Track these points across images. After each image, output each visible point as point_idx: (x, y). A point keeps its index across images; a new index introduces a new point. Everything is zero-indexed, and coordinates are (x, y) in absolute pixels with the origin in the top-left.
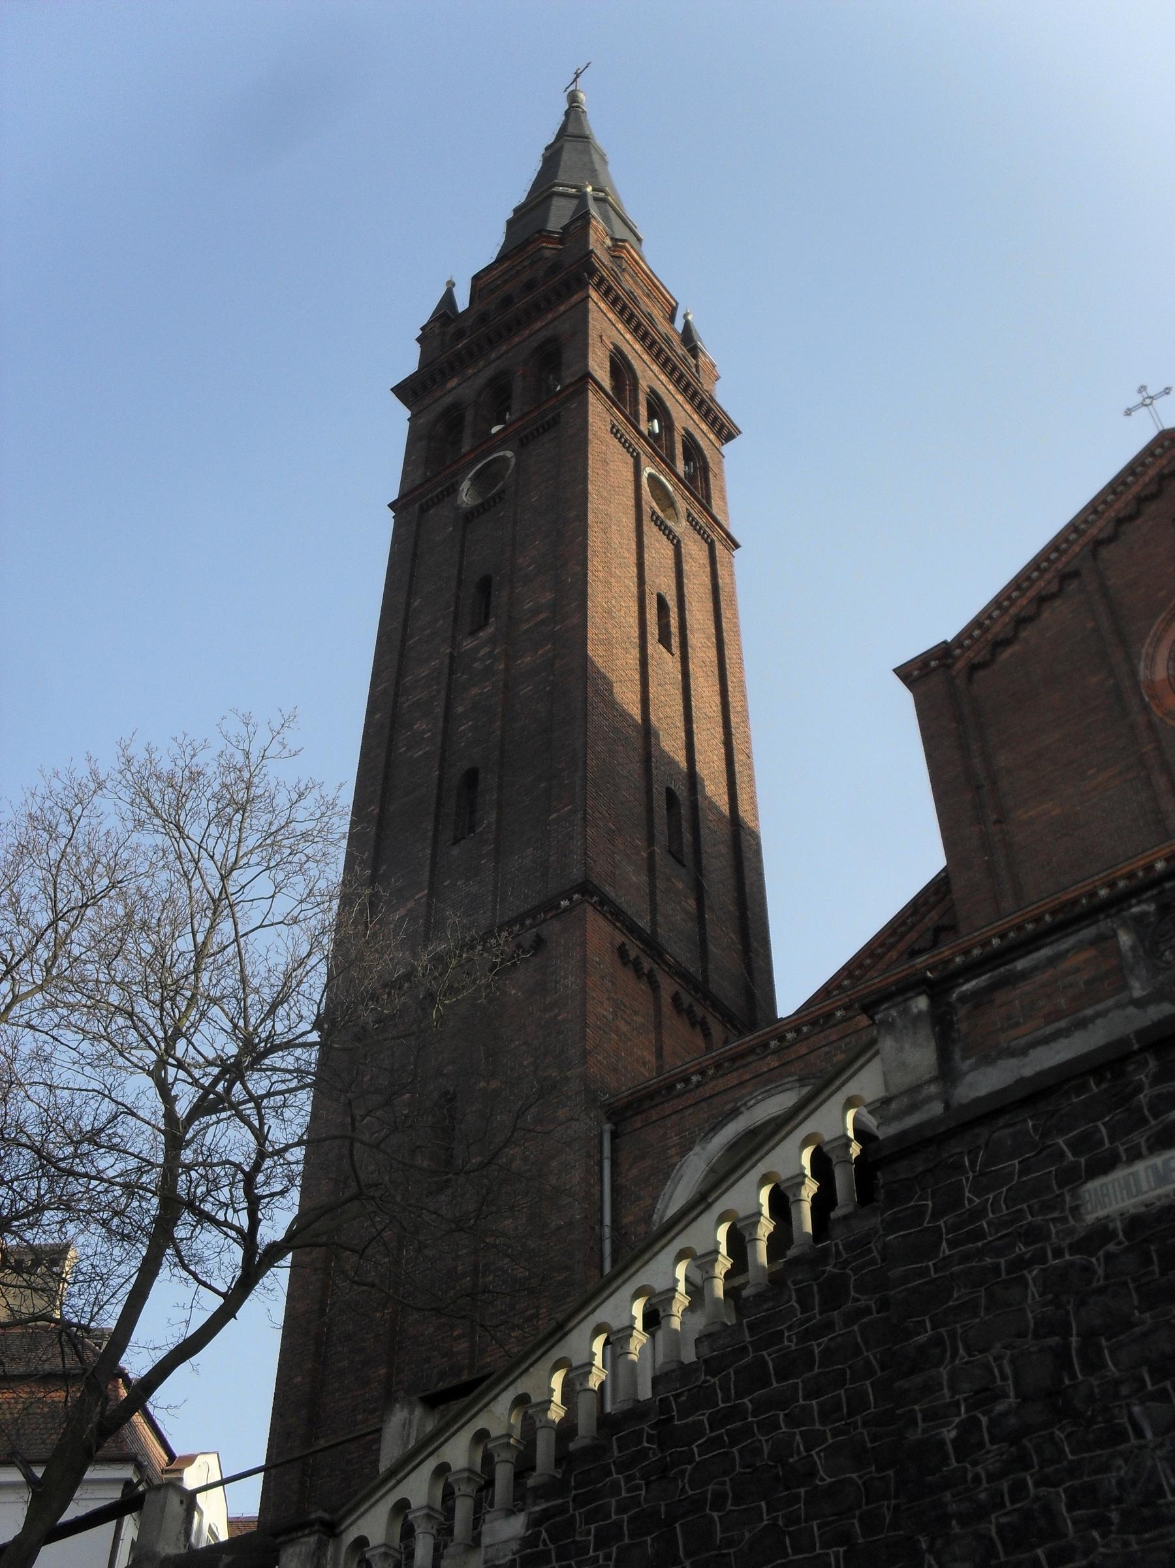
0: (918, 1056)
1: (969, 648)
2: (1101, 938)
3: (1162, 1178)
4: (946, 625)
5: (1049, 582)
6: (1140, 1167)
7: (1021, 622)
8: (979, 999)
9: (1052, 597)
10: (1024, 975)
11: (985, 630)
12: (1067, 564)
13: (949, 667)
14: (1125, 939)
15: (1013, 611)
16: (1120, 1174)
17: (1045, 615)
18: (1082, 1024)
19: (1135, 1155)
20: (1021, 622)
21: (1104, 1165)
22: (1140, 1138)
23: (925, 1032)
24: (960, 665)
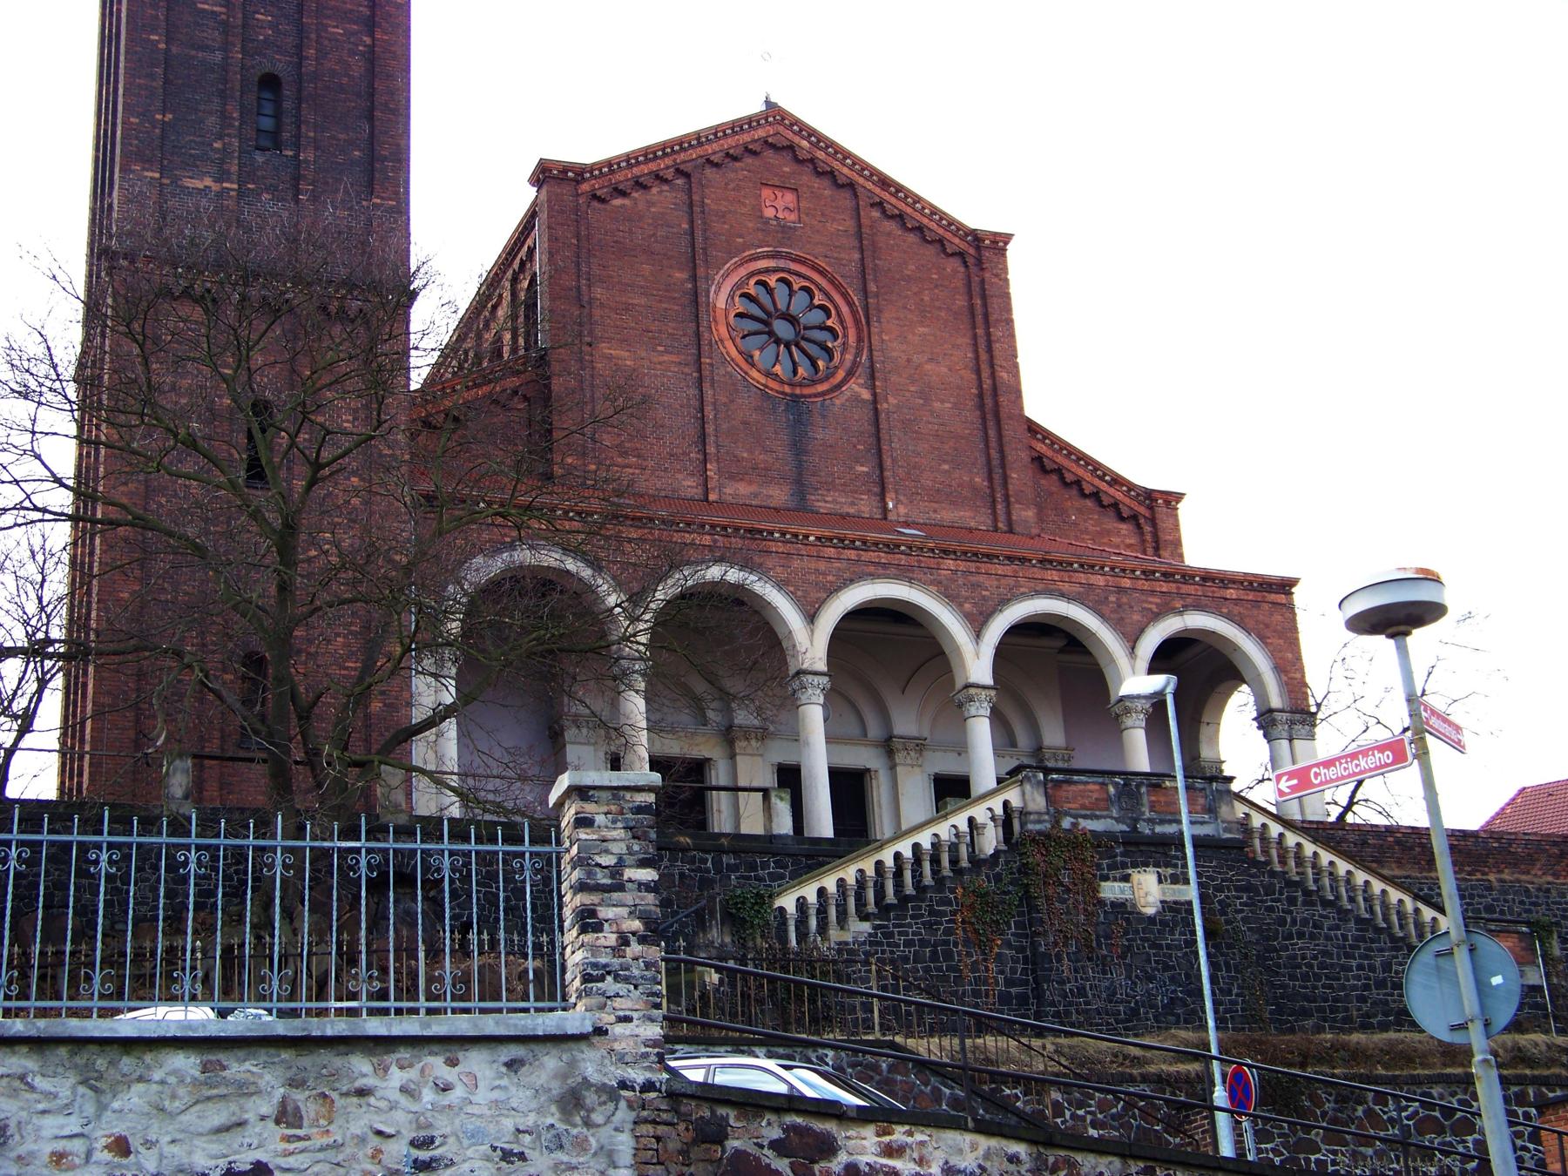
0: (1038, 802)
1: (596, 177)
2: (1103, 784)
3: (1122, 892)
4: (589, 146)
5: (667, 168)
6: (1116, 884)
7: (639, 185)
8: (1058, 783)
9: (666, 181)
10: (1076, 783)
11: (612, 172)
12: (684, 162)
13: (578, 182)
14: (1112, 790)
15: (636, 171)
16: (1108, 884)
17: (655, 190)
18: (1098, 817)
19: (1115, 880)
20: (639, 185)
21: (1106, 878)
22: (1117, 873)
23: (1042, 790)
24: (585, 187)
